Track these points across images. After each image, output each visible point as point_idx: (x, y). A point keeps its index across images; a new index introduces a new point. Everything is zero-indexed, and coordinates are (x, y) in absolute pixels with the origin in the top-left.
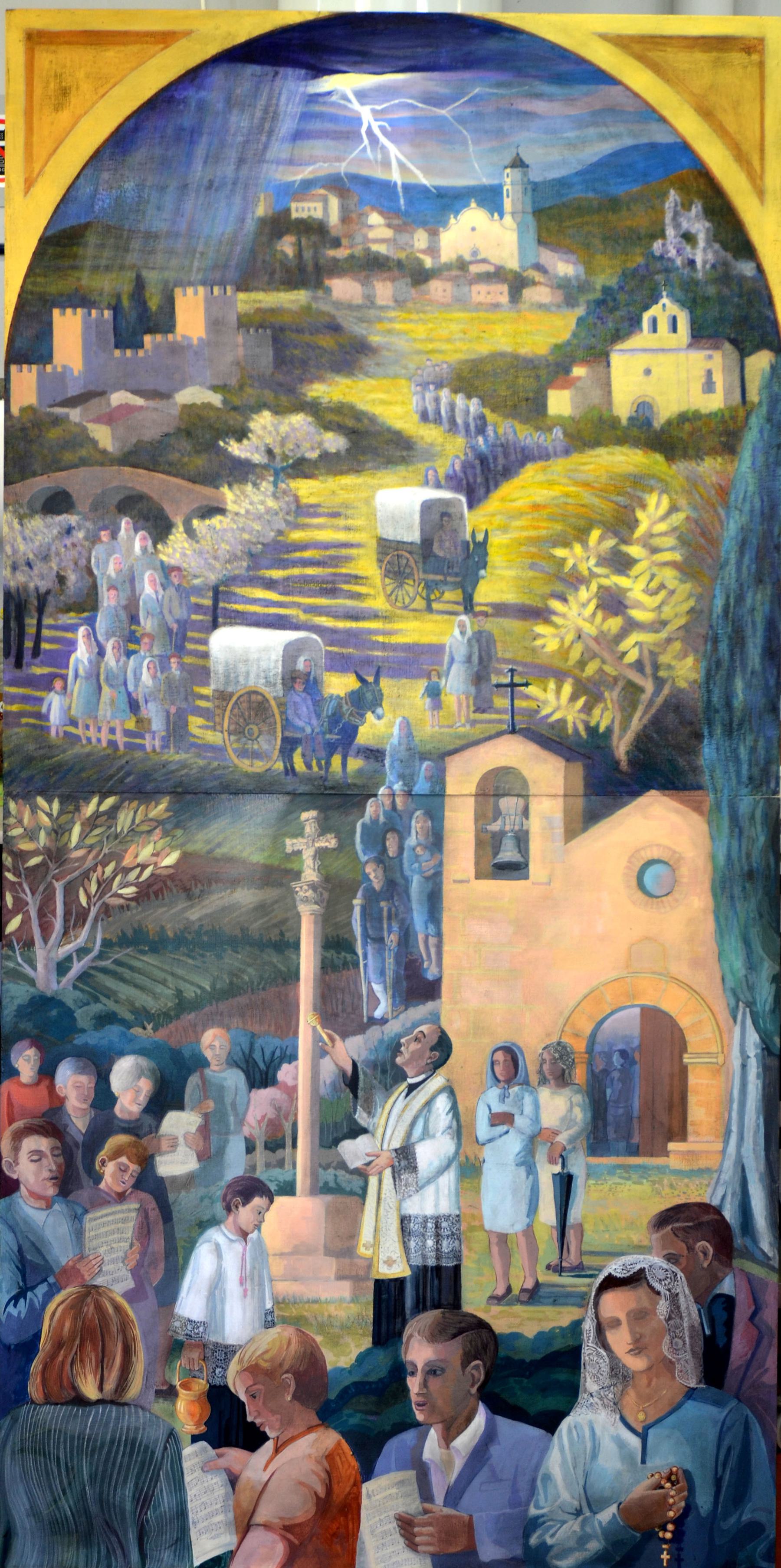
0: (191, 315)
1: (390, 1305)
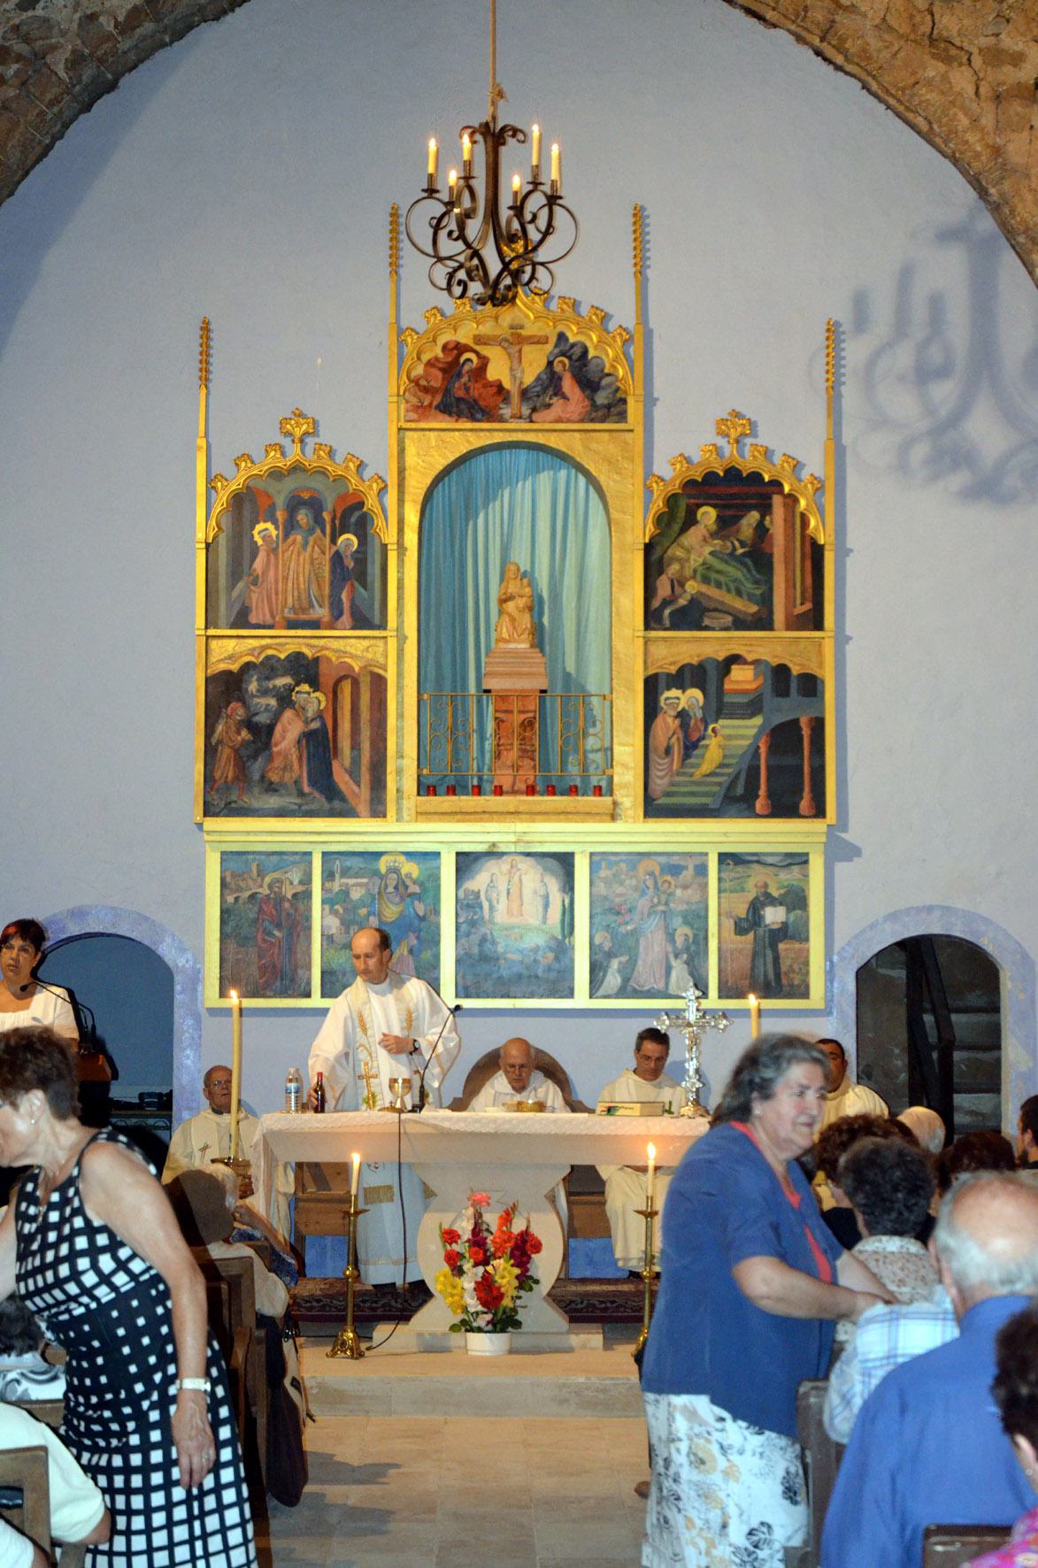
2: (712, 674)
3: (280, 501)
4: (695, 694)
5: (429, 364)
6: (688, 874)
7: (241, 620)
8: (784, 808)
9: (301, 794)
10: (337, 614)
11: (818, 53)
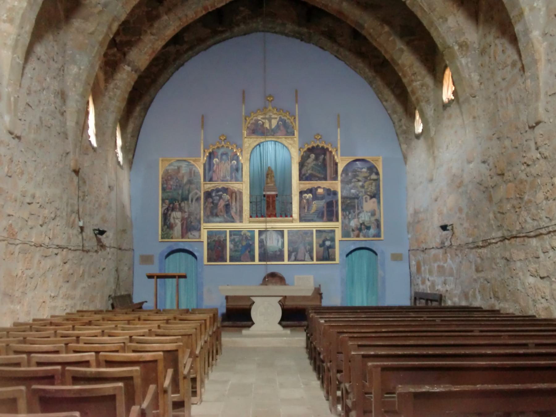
0: (350, 174)
1: (361, 224)
2: (314, 190)
3: (219, 154)
4: (310, 195)
5: (252, 124)
6: (309, 234)
7: (211, 180)
8: (330, 220)
9: (224, 218)
10: (232, 178)
11: (336, 56)
